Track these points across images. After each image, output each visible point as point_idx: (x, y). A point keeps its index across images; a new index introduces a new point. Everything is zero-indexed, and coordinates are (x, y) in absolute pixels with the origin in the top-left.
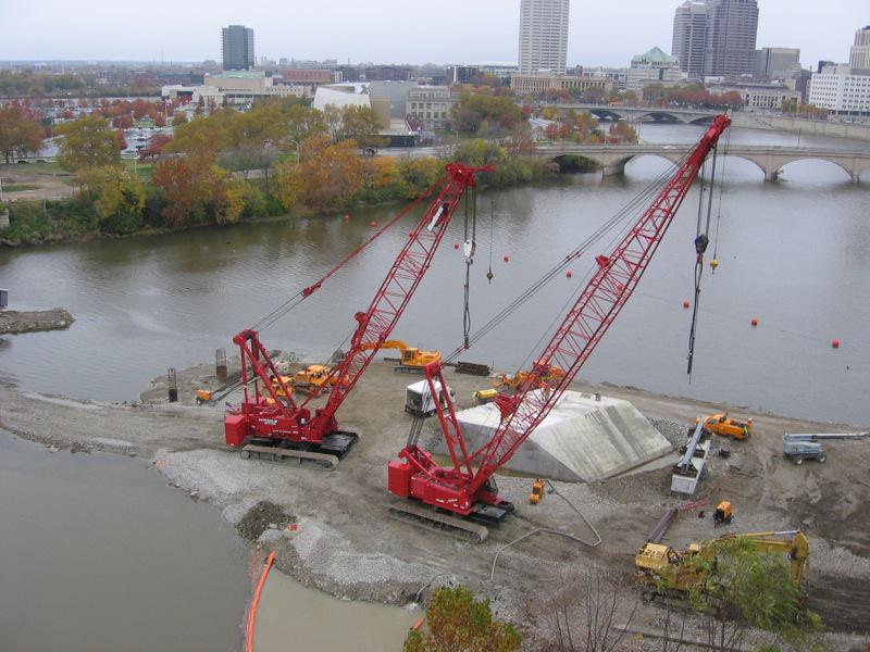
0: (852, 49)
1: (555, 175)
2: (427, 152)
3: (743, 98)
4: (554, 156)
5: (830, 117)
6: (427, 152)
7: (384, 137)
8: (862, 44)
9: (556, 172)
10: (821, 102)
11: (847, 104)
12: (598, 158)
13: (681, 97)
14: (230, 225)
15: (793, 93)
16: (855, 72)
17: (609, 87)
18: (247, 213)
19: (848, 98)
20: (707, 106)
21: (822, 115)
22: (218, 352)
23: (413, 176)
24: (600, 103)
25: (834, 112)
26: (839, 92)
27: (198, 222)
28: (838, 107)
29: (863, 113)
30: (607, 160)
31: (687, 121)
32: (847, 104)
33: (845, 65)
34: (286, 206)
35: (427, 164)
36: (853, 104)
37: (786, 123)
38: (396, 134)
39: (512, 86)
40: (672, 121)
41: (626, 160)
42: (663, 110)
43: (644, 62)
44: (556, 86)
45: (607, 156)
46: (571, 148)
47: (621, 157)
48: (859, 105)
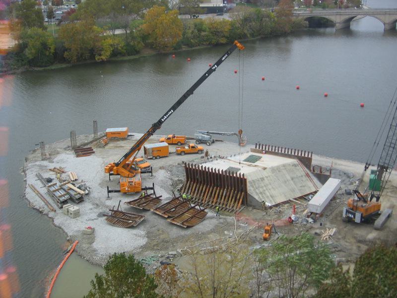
1: (306, 29)
2: (226, 17)
4: (305, 17)
6: (226, 17)
7: (203, 8)
9: (306, 27)
12: (333, 18)
14: (103, 63)
18: (115, 53)
22: (71, 133)
23: (216, 32)
27: (85, 59)
30: (337, 17)
34: (138, 50)
35: (224, 22)
38: (212, 6)
41: (351, 19)
45: (338, 17)
46: (318, 12)
47: (347, 17)
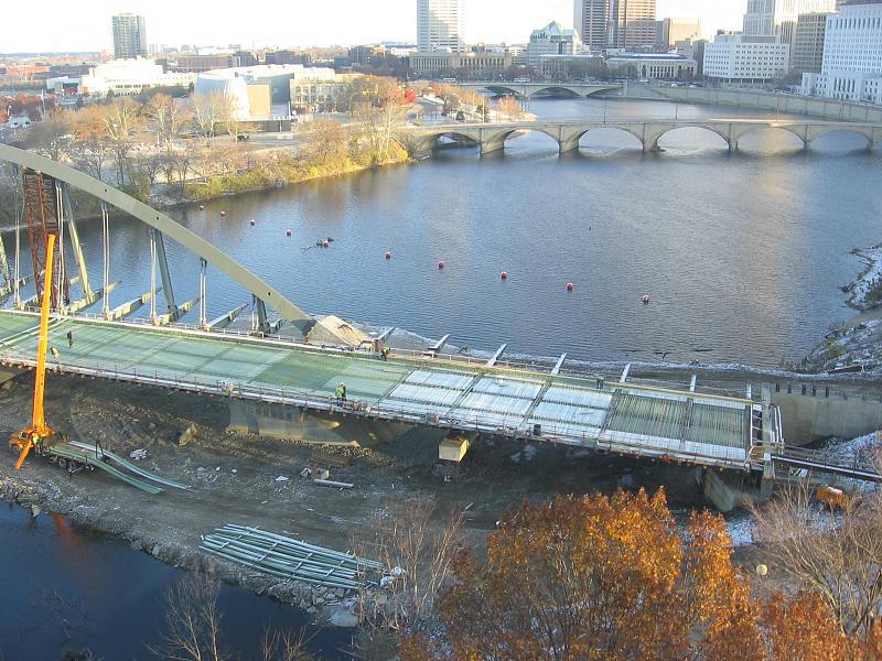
0: (745, 17)
3: (640, 69)
5: (723, 84)
8: (755, 11)
10: (717, 71)
11: (739, 72)
13: (576, 70)
15: (690, 62)
16: (745, 39)
17: (508, 63)
19: (739, 66)
20: (605, 79)
21: (716, 81)
24: (498, 79)
25: (727, 80)
26: (732, 60)
28: (730, 75)
29: (756, 80)
31: (585, 93)
32: (739, 72)
33: (739, 33)
36: (745, 72)
37: (681, 93)
39: (412, 65)
40: (572, 96)
42: (559, 84)
43: (543, 36)
44: (455, 64)
48: (751, 72)
